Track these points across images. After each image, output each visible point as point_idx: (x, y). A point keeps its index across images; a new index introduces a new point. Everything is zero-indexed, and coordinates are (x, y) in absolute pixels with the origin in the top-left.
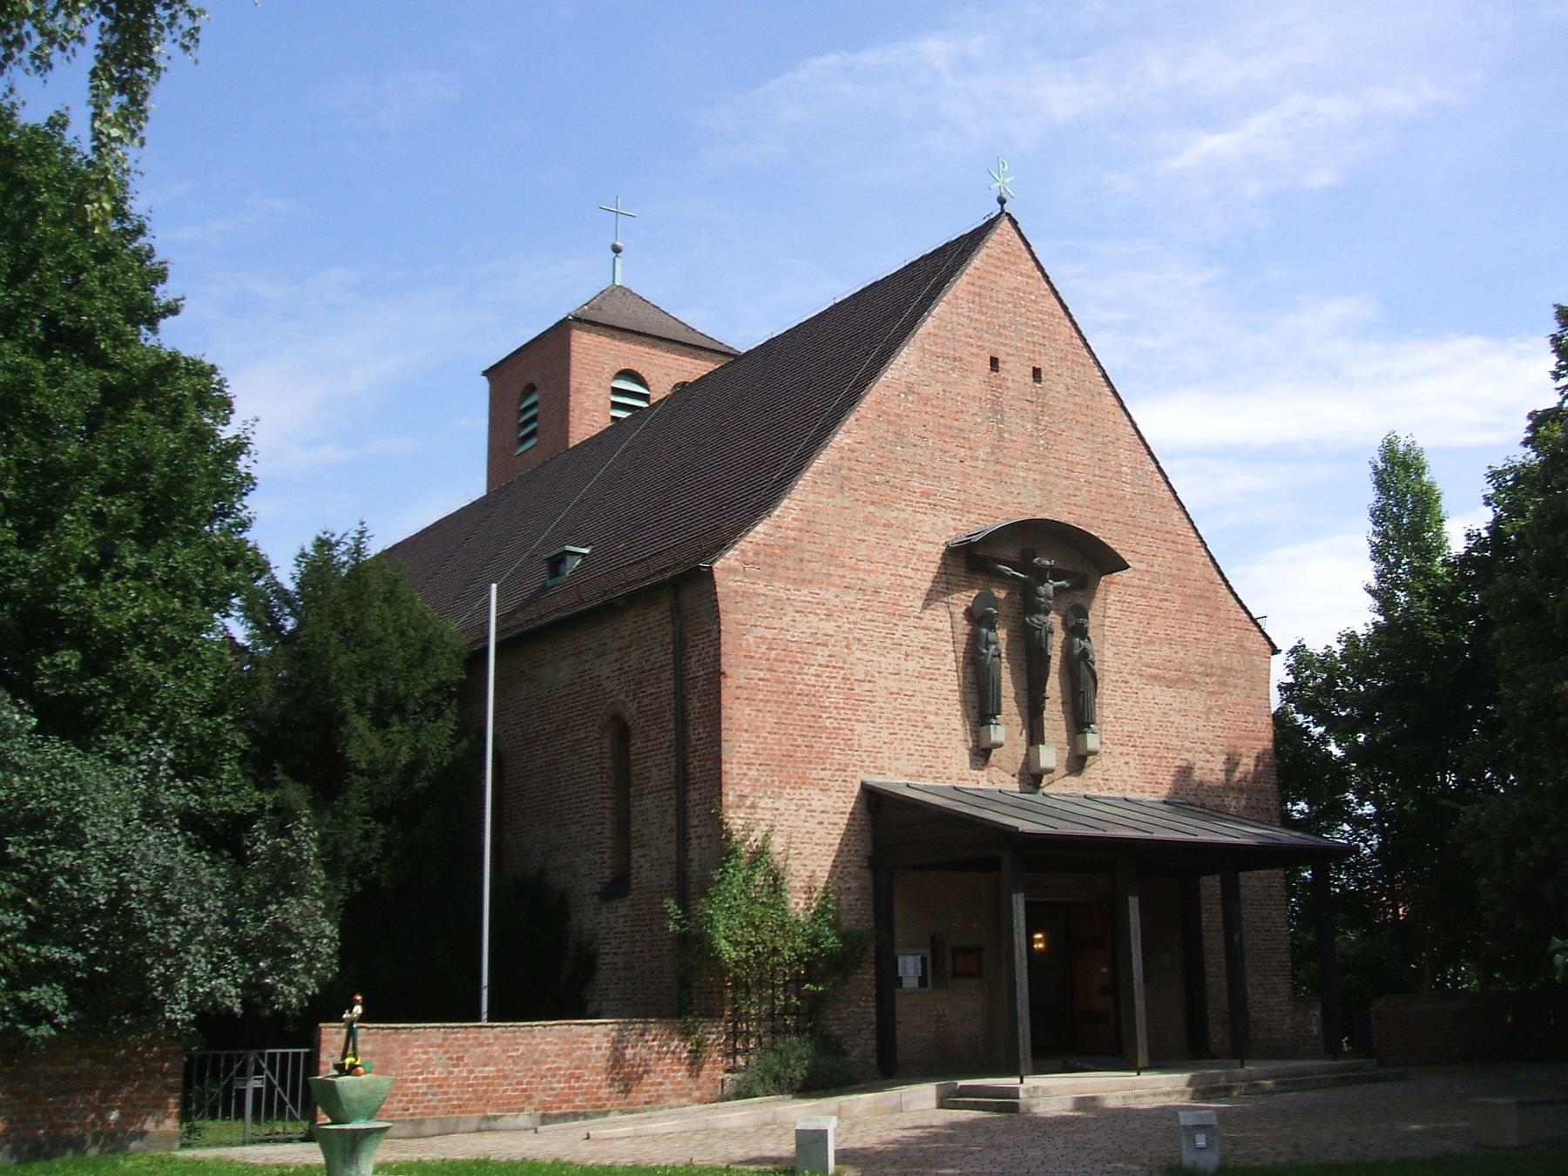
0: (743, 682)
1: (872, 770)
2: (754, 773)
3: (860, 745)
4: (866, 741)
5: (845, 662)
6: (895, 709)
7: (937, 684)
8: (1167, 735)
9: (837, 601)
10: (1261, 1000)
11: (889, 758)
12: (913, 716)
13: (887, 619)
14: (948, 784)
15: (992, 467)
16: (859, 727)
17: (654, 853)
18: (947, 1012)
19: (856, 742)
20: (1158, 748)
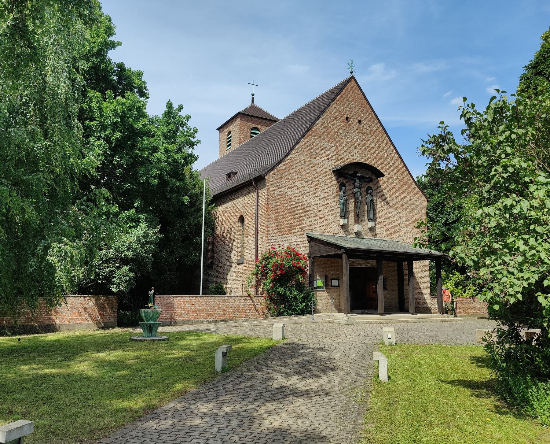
0: (273, 206)
6: (316, 214)
13: (314, 189)
14: (330, 234)
15: (346, 148)
16: (305, 219)
17: (250, 251)
19: (305, 223)
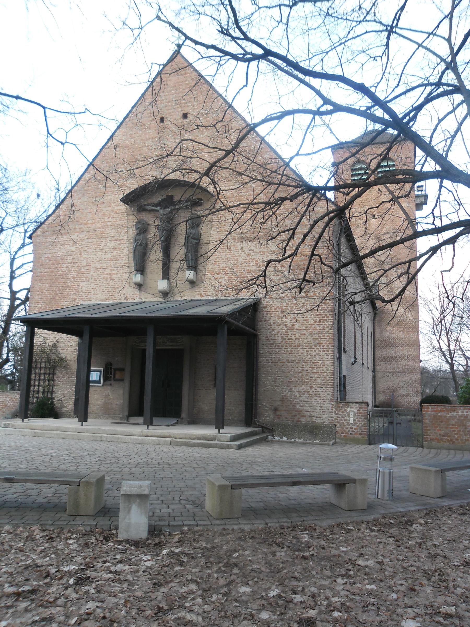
0: (39, 274)
2: (40, 306)
3: (82, 291)
4: (84, 289)
5: (78, 260)
6: (98, 275)
8: (249, 266)
9: (77, 238)
10: (306, 400)
11: (94, 294)
13: (98, 240)
16: (82, 284)
18: (110, 394)
19: (80, 290)
20: (242, 273)
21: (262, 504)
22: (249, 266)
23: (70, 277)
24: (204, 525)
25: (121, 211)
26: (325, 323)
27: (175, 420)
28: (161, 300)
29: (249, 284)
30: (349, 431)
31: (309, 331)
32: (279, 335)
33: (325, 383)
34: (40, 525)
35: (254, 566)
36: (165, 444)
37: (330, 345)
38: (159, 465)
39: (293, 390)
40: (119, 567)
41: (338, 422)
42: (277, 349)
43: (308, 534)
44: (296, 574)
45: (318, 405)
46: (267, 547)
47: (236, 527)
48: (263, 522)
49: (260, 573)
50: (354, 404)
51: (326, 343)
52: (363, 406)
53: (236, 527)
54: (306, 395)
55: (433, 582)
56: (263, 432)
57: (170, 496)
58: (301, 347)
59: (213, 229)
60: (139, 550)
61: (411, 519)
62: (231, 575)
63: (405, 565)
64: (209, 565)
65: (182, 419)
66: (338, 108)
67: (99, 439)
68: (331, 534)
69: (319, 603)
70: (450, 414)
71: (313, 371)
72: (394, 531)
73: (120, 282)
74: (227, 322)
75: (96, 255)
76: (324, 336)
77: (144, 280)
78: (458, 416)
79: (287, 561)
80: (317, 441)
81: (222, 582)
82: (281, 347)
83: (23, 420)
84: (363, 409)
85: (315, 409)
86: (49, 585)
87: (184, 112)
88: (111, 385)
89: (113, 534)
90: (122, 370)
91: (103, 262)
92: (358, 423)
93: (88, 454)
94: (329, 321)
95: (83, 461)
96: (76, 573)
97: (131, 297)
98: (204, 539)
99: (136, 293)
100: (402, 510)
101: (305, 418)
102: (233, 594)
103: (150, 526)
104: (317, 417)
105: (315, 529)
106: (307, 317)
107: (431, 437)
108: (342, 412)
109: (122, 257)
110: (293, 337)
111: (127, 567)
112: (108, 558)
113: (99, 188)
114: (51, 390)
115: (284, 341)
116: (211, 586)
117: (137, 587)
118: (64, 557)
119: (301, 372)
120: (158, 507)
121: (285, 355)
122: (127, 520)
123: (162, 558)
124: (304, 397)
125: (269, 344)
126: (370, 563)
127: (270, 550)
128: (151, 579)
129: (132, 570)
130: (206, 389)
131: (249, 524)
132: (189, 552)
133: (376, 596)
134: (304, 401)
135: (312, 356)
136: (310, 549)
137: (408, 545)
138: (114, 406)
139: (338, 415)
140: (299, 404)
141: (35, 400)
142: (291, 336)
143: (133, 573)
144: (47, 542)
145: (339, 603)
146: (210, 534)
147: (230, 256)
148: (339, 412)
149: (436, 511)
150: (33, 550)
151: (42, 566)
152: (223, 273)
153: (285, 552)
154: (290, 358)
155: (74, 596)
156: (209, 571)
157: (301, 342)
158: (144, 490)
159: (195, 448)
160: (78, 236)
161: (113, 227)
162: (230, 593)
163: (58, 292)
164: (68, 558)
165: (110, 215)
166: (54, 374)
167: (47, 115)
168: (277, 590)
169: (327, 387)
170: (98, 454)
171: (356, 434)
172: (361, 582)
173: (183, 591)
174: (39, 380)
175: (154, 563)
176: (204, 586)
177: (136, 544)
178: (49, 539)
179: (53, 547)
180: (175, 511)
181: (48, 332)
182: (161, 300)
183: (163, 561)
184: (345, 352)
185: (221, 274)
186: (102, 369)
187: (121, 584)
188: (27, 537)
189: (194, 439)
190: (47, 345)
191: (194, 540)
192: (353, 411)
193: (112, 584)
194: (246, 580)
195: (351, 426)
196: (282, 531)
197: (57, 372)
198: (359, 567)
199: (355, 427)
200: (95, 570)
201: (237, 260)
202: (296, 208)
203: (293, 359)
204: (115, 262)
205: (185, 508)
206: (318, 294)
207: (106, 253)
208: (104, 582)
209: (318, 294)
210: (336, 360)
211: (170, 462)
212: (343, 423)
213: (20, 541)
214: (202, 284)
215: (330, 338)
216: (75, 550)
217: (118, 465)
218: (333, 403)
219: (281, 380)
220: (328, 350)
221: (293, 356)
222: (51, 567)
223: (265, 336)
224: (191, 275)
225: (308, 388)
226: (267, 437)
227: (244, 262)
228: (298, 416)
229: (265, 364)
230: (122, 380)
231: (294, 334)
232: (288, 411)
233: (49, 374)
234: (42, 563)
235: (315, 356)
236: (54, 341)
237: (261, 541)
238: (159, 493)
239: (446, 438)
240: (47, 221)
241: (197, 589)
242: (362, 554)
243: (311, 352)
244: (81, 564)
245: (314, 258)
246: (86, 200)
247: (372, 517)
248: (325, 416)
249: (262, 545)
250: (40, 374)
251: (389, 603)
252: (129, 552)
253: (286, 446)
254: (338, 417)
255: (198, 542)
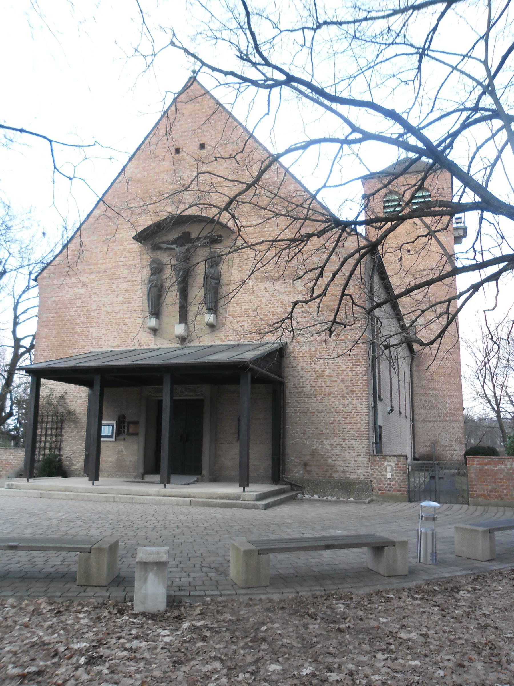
0: (45, 319)
1: (96, 346)
2: (46, 354)
3: (91, 337)
4: (94, 335)
5: (88, 303)
6: (109, 319)
7: (132, 305)
8: (274, 307)
9: (87, 280)
10: (339, 453)
11: (105, 341)
12: (118, 321)
13: (109, 281)
16: (91, 330)
19: (90, 336)
20: (266, 315)
21: (292, 571)
22: (273, 307)
23: (79, 322)
24: (229, 595)
25: (133, 250)
26: (358, 369)
27: (195, 478)
28: (178, 346)
29: (274, 327)
30: (386, 487)
31: (341, 377)
32: (308, 382)
33: (359, 434)
34: (47, 597)
35: (285, 641)
36: (184, 504)
37: (364, 393)
38: (178, 528)
39: (325, 442)
40: (135, 644)
41: (375, 478)
42: (305, 397)
43: (343, 604)
44: (331, 649)
45: (351, 459)
46: (299, 618)
47: (263, 597)
48: (293, 591)
49: (291, 648)
50: (392, 457)
51: (360, 391)
52: (402, 460)
53: (263, 597)
54: (338, 448)
55: (484, 656)
56: (292, 490)
57: (190, 562)
58: (332, 395)
59: (234, 268)
60: (157, 625)
61: (458, 585)
62: (259, 651)
63: (452, 637)
64: (234, 640)
65: (203, 476)
66: (367, 136)
67: (112, 500)
68: (369, 604)
69: (358, 682)
70: (498, 467)
71: (346, 422)
72: (439, 599)
73: (133, 327)
74: (251, 369)
75: (107, 298)
76: (357, 383)
77: (160, 324)
78: (506, 470)
79: (321, 634)
80: (352, 499)
81: (249, 659)
82: (310, 396)
83: (28, 480)
84: (402, 463)
85: (349, 464)
86: (57, 665)
87: (201, 142)
88: (124, 439)
89: (128, 606)
90: (136, 423)
91: (114, 305)
92: (397, 478)
93: (99, 517)
94: (363, 366)
95: (94, 525)
96: (87, 651)
97: (145, 343)
98: (229, 610)
99: (150, 338)
100: (447, 575)
101: (337, 474)
102: (261, 673)
103: (168, 596)
104: (351, 472)
105: (351, 598)
106: (338, 363)
107: (477, 492)
108: (379, 467)
109: (136, 300)
110: (323, 384)
111: (144, 643)
112: (123, 634)
113: (109, 226)
114: (58, 446)
115: (313, 389)
116: (237, 665)
117: (155, 666)
118: (74, 633)
119: (333, 423)
120: (177, 575)
121: (314, 405)
122: (143, 591)
123: (183, 633)
124: (337, 451)
125: (297, 393)
126: (413, 635)
127: (302, 623)
128: (170, 657)
129: (149, 647)
130: (228, 444)
131: (279, 593)
132: (213, 626)
133: (421, 673)
134: (337, 455)
135: (344, 405)
136: (347, 621)
137: (455, 615)
138: (128, 463)
139: (375, 470)
140: (331, 458)
141: (41, 457)
142: (321, 384)
143: (151, 650)
144: (55, 617)
145: (380, 682)
146: (235, 605)
147: (253, 297)
148: (376, 466)
149: (485, 577)
150: (39, 626)
151: (49, 643)
152: (246, 315)
153: (319, 624)
154: (321, 408)
155: (85, 677)
156: (234, 647)
157: (332, 390)
158: (162, 557)
159: (217, 508)
160: (87, 277)
161: (126, 267)
162: (258, 672)
163: (66, 339)
164: (78, 635)
165: (122, 254)
166: (61, 428)
167: (53, 149)
168: (311, 668)
169: (361, 439)
170: (110, 516)
171: (394, 490)
172: (404, 658)
173: (205, 669)
174: (46, 435)
175: (174, 639)
176: (229, 664)
177: (154, 617)
178: (57, 613)
179: (62, 622)
180: (196, 579)
181: (55, 382)
182: (178, 346)
183: (183, 636)
184: (381, 400)
185: (244, 316)
186: (114, 422)
187: (137, 662)
188: (33, 611)
189: (216, 498)
190: (54, 397)
191: (218, 612)
192: (391, 465)
193: (128, 663)
194: (276, 657)
195: (389, 482)
196: (315, 600)
197: (65, 426)
198: (401, 641)
199: (394, 483)
200: (109, 648)
201: (261, 301)
202: (324, 245)
203: (324, 409)
204: (127, 305)
205: (207, 576)
206: (349, 337)
207: (117, 295)
208: (118, 661)
209: (349, 337)
210: (371, 409)
211: (190, 525)
212: (380, 478)
213: (25, 615)
214: (223, 328)
215: (363, 385)
216: (86, 625)
217: (133, 529)
218: (368, 457)
219: (311, 432)
220: (362, 398)
221: (324, 406)
222: (59, 644)
223: (292, 384)
224: (210, 318)
225: (341, 440)
226: (296, 496)
227: (269, 303)
228: (330, 472)
229: (293, 414)
230: (136, 434)
231: (324, 382)
232: (319, 466)
233: (57, 429)
234: (50, 640)
235: (348, 405)
236: (62, 392)
237: (291, 612)
238: (178, 559)
239: (493, 493)
240: (54, 262)
241: (222, 667)
242: (404, 625)
243: (343, 401)
244: (93, 641)
245: (344, 298)
246: (95, 238)
247: (415, 583)
248: (360, 471)
249: (293, 617)
250: (47, 429)
251: (435, 681)
252: (146, 626)
253: (318, 505)
254: (374, 472)
255: (222, 614)
